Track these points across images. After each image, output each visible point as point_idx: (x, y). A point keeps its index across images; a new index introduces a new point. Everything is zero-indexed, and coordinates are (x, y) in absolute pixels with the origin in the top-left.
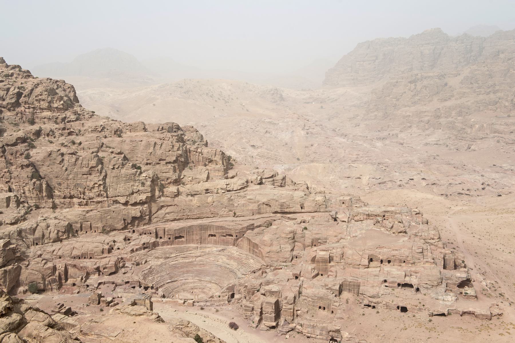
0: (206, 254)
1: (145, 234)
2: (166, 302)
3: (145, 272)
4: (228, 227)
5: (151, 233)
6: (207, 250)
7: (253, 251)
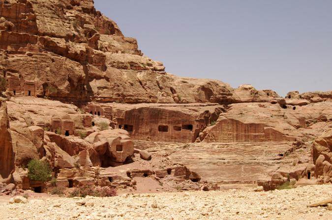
4: (185, 113)
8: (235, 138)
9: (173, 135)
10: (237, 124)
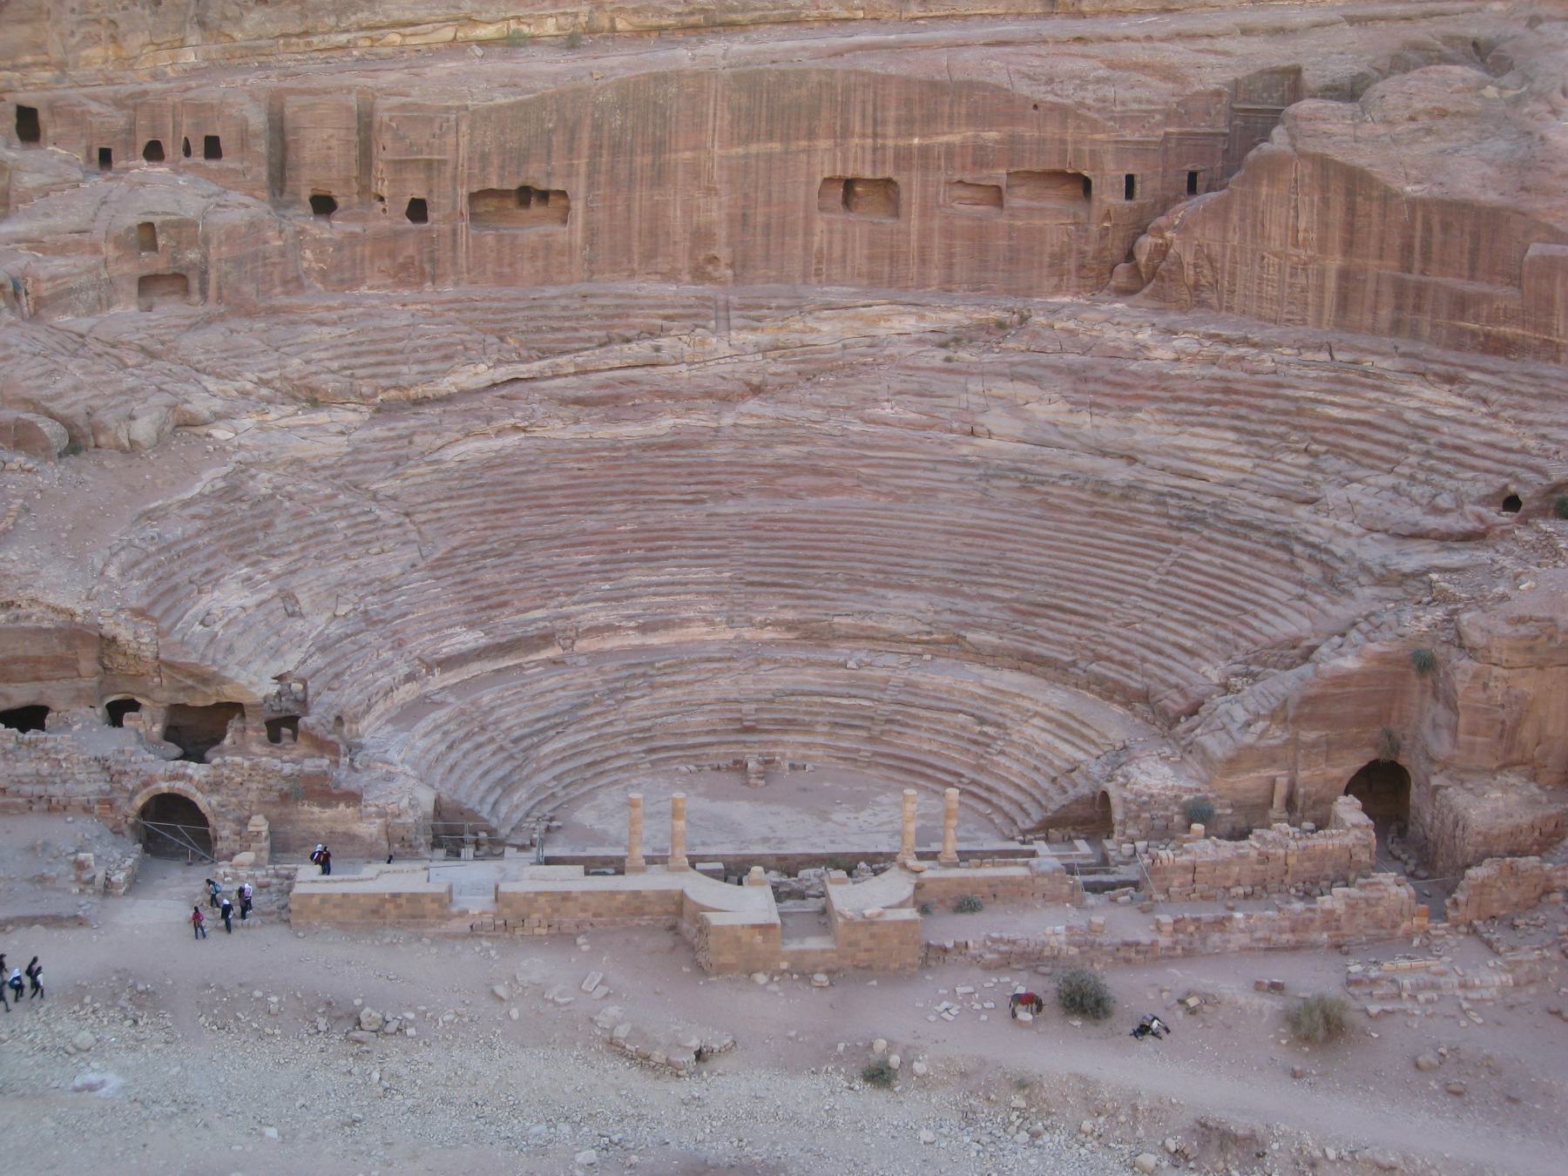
0: (814, 369)
1: (154, 152)
2: (511, 921)
3: (176, 531)
4: (1041, 93)
5: (213, 148)
6: (827, 332)
7: (1410, 299)
8: (1330, 298)
9: (937, 241)
10: (1350, 193)
